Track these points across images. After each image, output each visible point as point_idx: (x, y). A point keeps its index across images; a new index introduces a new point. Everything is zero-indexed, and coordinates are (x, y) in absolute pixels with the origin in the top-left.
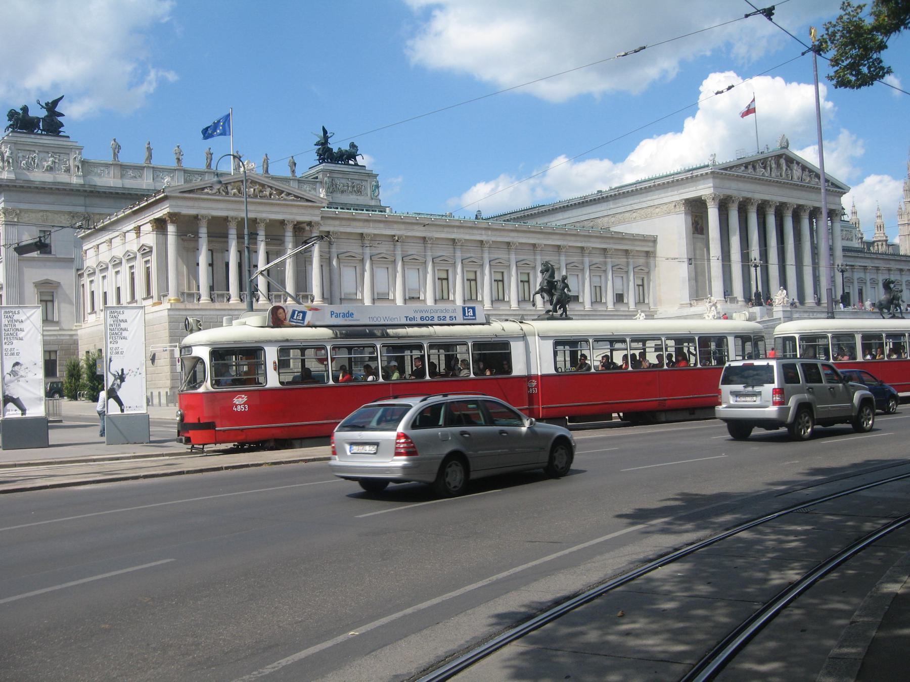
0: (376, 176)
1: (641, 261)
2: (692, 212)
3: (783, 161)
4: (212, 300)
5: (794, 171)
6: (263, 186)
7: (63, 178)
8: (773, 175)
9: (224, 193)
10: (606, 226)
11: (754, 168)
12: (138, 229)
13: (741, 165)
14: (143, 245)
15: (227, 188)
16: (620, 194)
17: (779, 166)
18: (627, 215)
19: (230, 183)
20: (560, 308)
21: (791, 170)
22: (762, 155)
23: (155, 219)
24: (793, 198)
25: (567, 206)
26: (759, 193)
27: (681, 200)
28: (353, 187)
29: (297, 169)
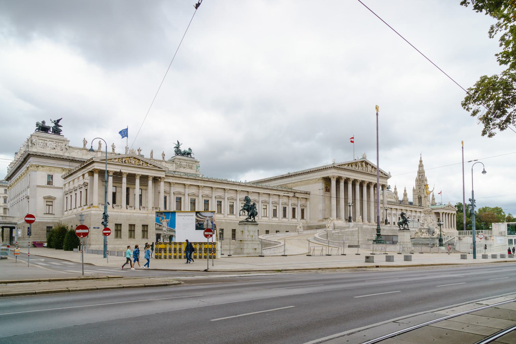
0: (198, 162)
1: (303, 202)
2: (325, 183)
3: (364, 164)
4: (113, 207)
5: (368, 168)
6: (139, 160)
7: (61, 153)
8: (359, 169)
9: (121, 162)
10: (291, 187)
11: (352, 166)
12: (83, 175)
13: (346, 164)
14: (84, 182)
15: (122, 160)
16: (297, 174)
17: (362, 165)
18: (299, 183)
19: (124, 158)
20: (252, 217)
21: (367, 167)
22: (355, 161)
23: (89, 171)
24: (367, 179)
25: (276, 178)
26: (353, 176)
27: (321, 178)
28: (189, 166)
29: (165, 157)
